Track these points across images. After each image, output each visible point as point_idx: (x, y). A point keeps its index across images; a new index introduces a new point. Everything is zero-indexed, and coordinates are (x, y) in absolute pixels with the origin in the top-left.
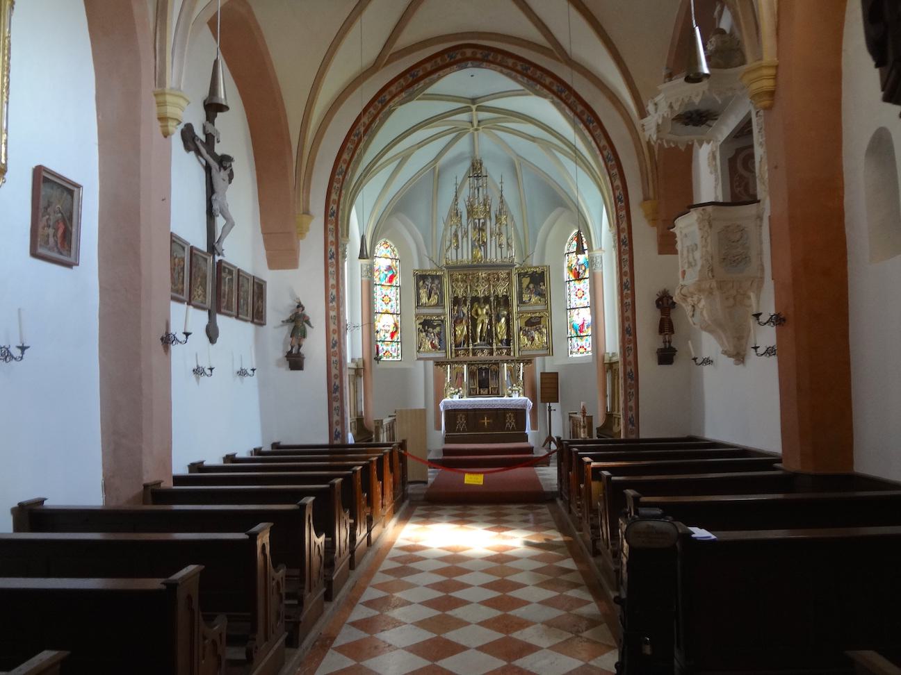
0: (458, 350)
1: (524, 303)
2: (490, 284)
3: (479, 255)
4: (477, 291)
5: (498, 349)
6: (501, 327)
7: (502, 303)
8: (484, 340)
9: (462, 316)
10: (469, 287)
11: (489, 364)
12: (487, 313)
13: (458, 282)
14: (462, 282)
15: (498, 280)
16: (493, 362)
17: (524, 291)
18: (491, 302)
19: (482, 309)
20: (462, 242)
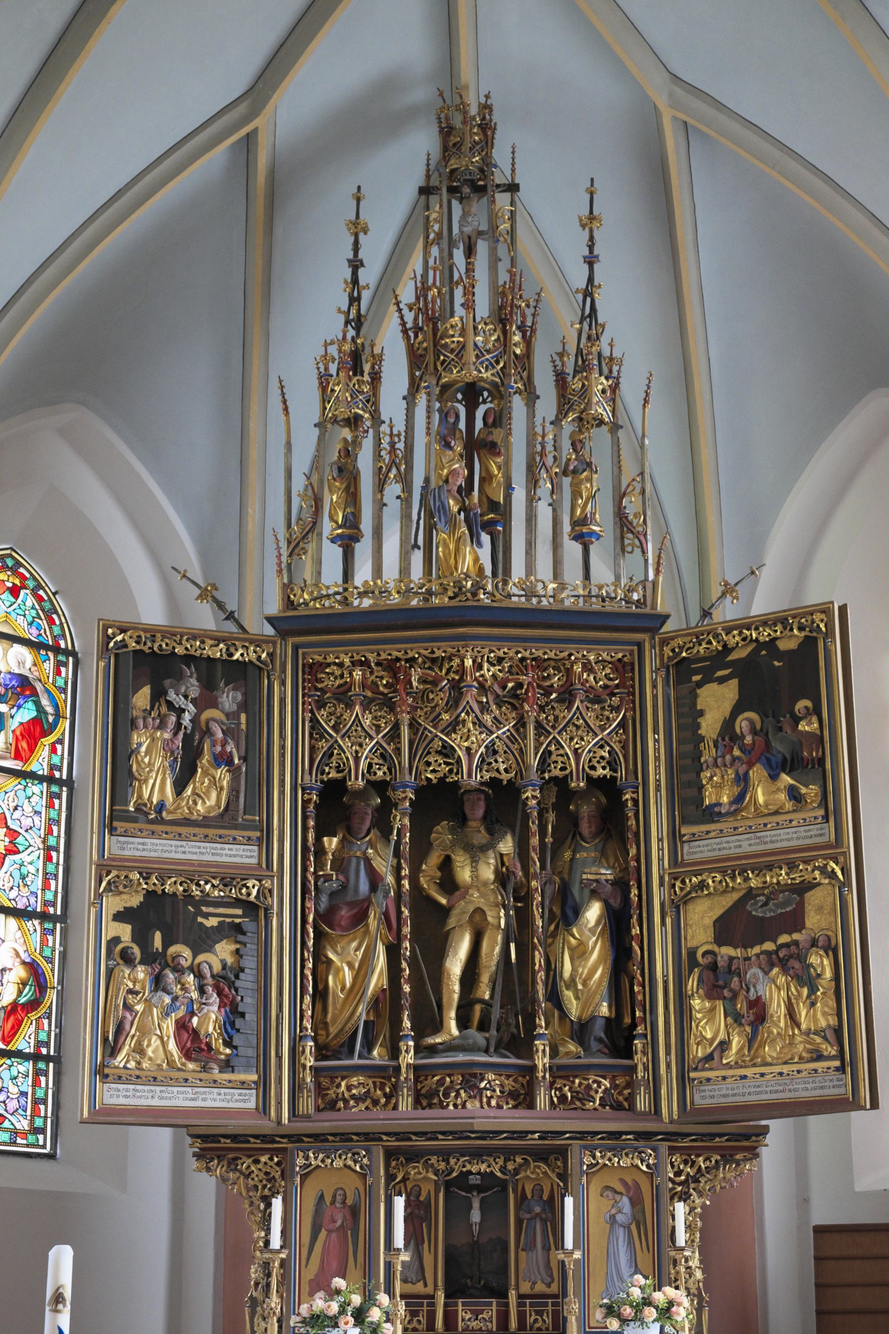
0: (335, 1075)
1: (711, 814)
2: (521, 723)
3: (467, 563)
4: (447, 751)
5: (560, 1072)
6: (580, 953)
7: (585, 828)
8: (483, 1026)
9: (364, 886)
10: (405, 732)
11: (509, 1153)
12: (502, 879)
13: (349, 706)
14: (365, 707)
15: (567, 696)
16: (534, 1140)
17: (708, 755)
18: (526, 817)
19: (475, 853)
20: (380, 505)
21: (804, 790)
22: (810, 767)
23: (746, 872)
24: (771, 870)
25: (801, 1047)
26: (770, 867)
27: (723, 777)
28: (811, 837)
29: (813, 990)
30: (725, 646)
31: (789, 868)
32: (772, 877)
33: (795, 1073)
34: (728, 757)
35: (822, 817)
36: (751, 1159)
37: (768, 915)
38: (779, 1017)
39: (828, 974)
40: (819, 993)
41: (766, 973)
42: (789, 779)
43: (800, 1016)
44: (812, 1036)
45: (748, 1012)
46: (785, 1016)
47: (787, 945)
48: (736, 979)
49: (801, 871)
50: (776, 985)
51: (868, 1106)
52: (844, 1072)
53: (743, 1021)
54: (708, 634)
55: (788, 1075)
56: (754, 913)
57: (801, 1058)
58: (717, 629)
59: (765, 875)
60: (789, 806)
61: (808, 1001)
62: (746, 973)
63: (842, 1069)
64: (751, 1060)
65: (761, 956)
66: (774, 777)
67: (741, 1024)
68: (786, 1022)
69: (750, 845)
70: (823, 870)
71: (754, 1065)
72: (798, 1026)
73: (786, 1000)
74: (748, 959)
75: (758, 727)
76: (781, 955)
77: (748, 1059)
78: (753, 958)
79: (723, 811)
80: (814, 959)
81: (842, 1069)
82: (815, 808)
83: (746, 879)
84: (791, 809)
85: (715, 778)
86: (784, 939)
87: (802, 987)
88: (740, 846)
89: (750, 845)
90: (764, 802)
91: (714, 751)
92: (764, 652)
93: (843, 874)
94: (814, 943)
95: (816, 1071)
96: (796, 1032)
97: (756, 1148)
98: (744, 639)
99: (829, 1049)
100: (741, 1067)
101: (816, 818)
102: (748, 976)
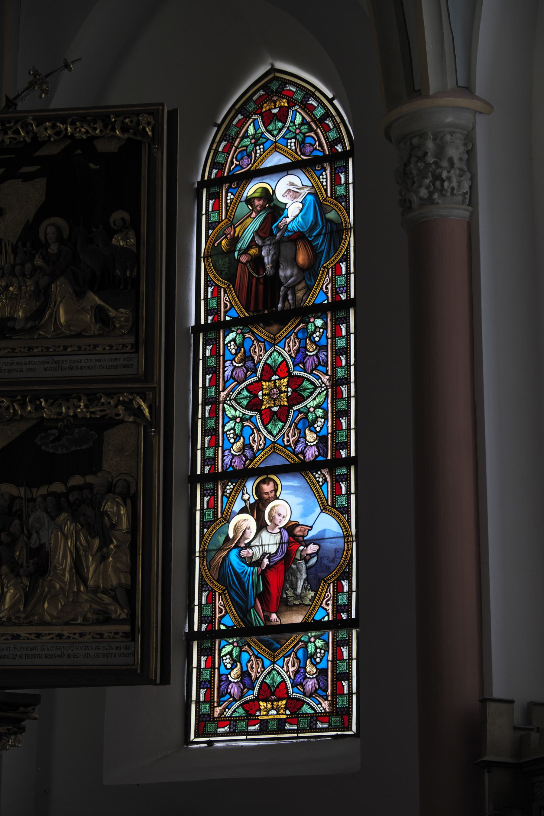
21: (112, 313)
22: (122, 287)
23: (39, 399)
24: (68, 400)
25: (86, 607)
26: (67, 397)
27: (20, 287)
28: (117, 367)
29: (105, 542)
30: (35, 138)
31: (88, 400)
32: (68, 408)
33: (77, 636)
34: (28, 266)
35: (132, 345)
36: (15, 734)
37: (60, 452)
38: (64, 570)
39: (125, 525)
40: (112, 546)
41: (53, 518)
42: (97, 298)
43: (88, 571)
44: (100, 595)
45: (27, 562)
46: (71, 569)
47: (79, 488)
48: (17, 522)
49: (103, 404)
50: (63, 533)
51: (158, 681)
52: (134, 639)
53: (21, 571)
54: (16, 123)
55: (69, 637)
56: (43, 448)
57: (85, 619)
58: (27, 117)
59: (60, 406)
60: (94, 329)
61: (99, 554)
62: (29, 516)
63: (131, 636)
64: (26, 618)
65: (49, 498)
66: (80, 295)
67: (18, 575)
68: (71, 577)
69: (46, 369)
70: (128, 405)
71: (30, 624)
72: (85, 582)
73: (73, 550)
74: (32, 500)
75: (66, 235)
76: (71, 499)
77: (23, 616)
78: (39, 500)
79: (17, 327)
80: (108, 507)
81: (131, 636)
82: (124, 334)
83: (39, 408)
84: (97, 333)
85: (11, 289)
86: (76, 480)
87: (93, 537)
88: (33, 370)
89: (46, 369)
90: (67, 321)
91: (12, 257)
92: (79, 152)
93: (150, 412)
94: (111, 488)
95: (101, 635)
96: (82, 589)
97: (23, 720)
98: (58, 133)
99: (119, 611)
100: (14, 624)
101: (124, 346)
102: (31, 520)
